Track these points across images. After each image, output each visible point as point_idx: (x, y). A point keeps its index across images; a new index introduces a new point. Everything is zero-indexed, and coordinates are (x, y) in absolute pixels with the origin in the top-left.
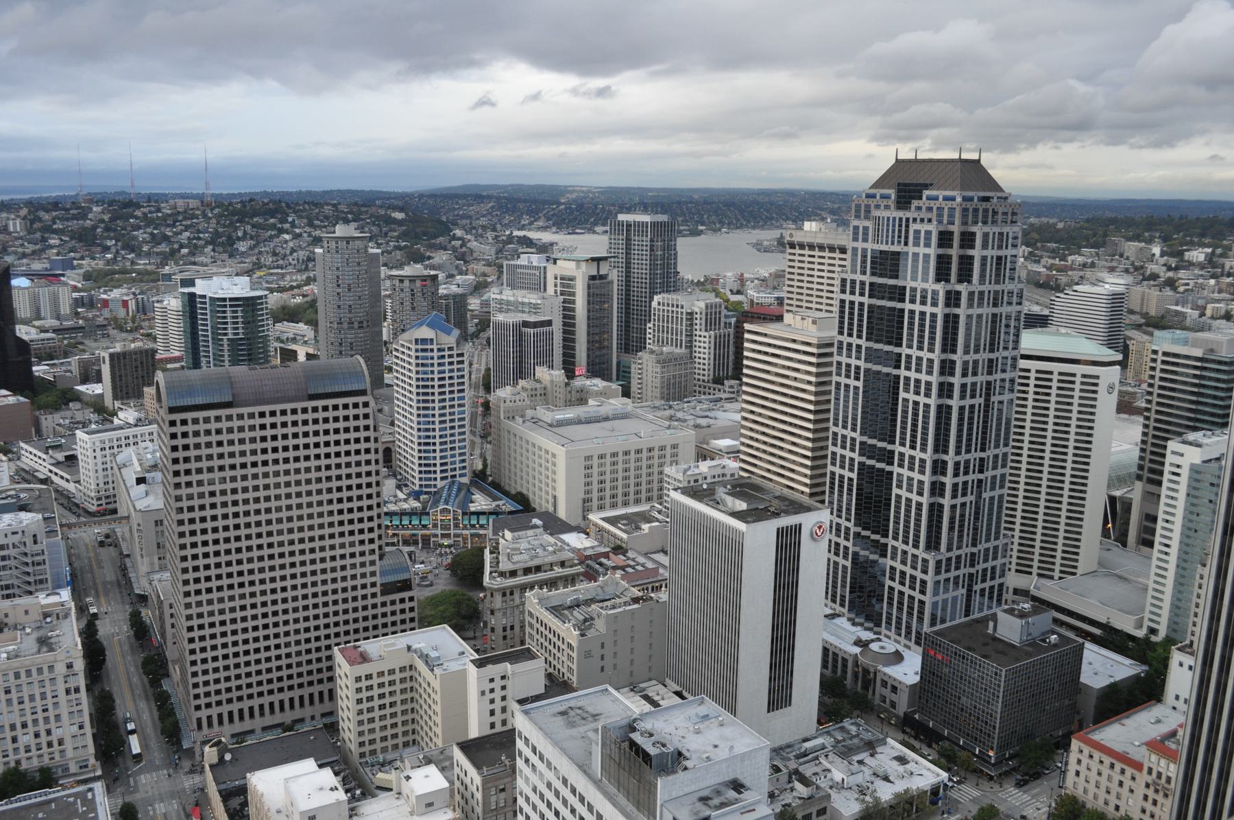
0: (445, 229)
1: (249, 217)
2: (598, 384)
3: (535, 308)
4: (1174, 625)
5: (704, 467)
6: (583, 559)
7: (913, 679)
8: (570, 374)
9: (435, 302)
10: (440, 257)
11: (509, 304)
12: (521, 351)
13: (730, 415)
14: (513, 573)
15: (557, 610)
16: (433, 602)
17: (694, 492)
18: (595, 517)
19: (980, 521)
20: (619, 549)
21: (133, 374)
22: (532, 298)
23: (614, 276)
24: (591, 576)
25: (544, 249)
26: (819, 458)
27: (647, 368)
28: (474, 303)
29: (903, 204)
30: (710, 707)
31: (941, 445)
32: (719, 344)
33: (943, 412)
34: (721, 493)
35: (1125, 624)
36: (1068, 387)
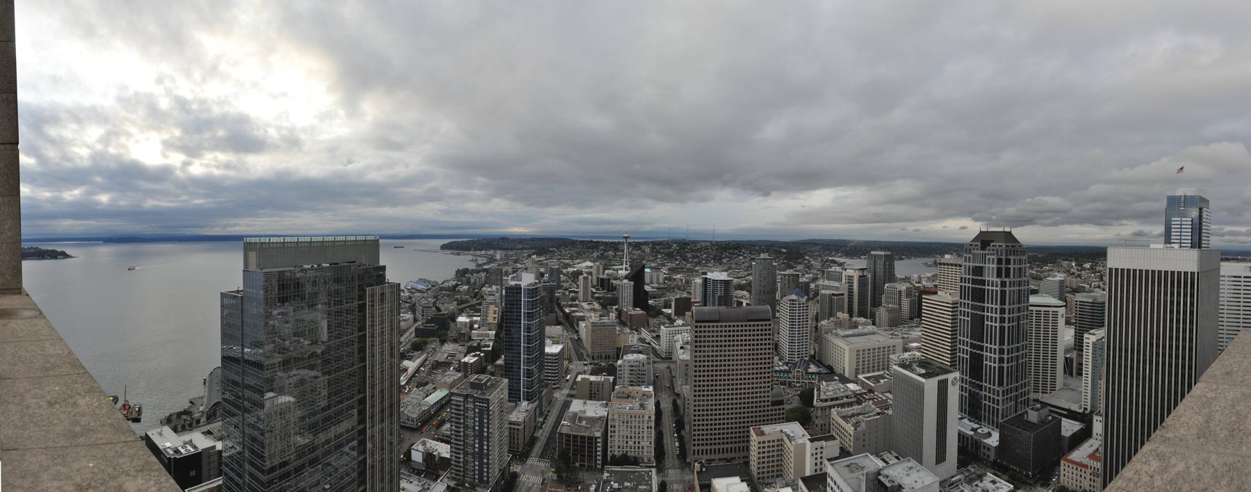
0: (802, 256)
1: (727, 250)
2: (863, 320)
3: (837, 288)
4: (1093, 406)
5: (906, 355)
6: (855, 394)
7: (996, 444)
8: (851, 316)
9: (798, 284)
10: (800, 267)
11: (827, 287)
12: (830, 306)
13: (916, 333)
14: (826, 400)
15: (844, 418)
16: (792, 411)
17: (903, 366)
18: (860, 377)
19: (1019, 372)
20: (871, 391)
21: (683, 306)
22: (836, 284)
23: (869, 276)
24: (859, 403)
25: (840, 265)
26: (953, 350)
27: (882, 313)
28: (812, 286)
30: (913, 463)
31: (1002, 343)
32: (912, 303)
34: (914, 366)
35: (1075, 408)
36: (1047, 316)
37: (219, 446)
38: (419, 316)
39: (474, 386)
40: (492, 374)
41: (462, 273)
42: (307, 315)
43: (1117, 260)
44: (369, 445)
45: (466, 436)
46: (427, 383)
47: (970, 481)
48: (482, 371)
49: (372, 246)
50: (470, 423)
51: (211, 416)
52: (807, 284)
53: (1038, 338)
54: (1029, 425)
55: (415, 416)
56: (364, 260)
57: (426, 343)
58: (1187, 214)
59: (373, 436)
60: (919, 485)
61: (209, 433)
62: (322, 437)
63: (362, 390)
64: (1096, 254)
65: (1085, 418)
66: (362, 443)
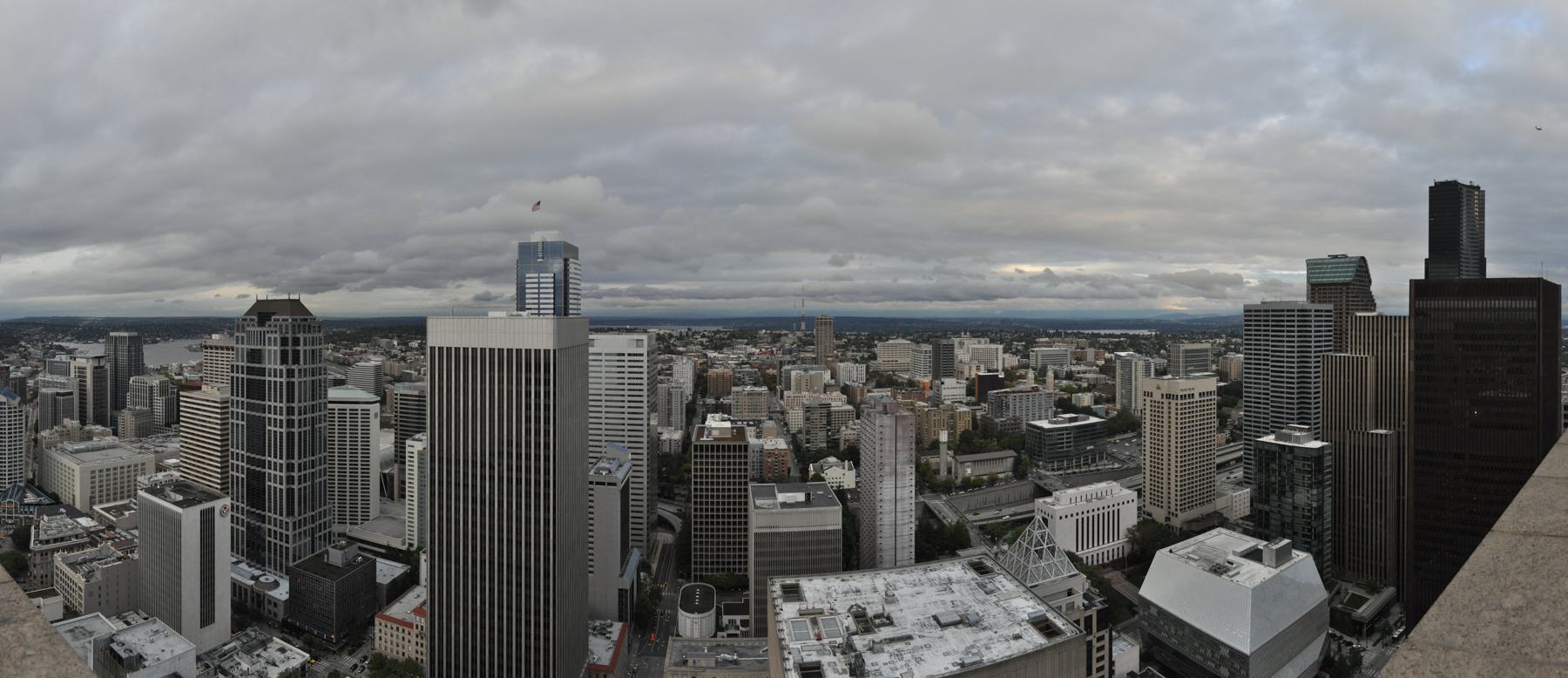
0: (16, 341)
2: (99, 428)
3: (63, 385)
5: (160, 476)
6: (89, 532)
7: (285, 597)
8: (83, 422)
10: (12, 357)
11: (49, 383)
12: (55, 410)
13: (174, 445)
14: (47, 542)
15: (72, 565)
17: (152, 490)
18: (97, 508)
20: (111, 527)
22: (62, 379)
23: (108, 366)
24: (93, 544)
25: (70, 352)
26: (224, 467)
27: (127, 418)
28: (31, 383)
29: (261, 324)
31: (290, 455)
32: (168, 404)
33: (290, 435)
34: (168, 490)
35: (396, 544)
36: (353, 417)
43: (440, 335)
47: (249, 650)
52: (23, 381)
53: (342, 448)
54: (332, 570)
58: (548, 268)
60: (167, 656)
64: (413, 328)
65: (407, 557)
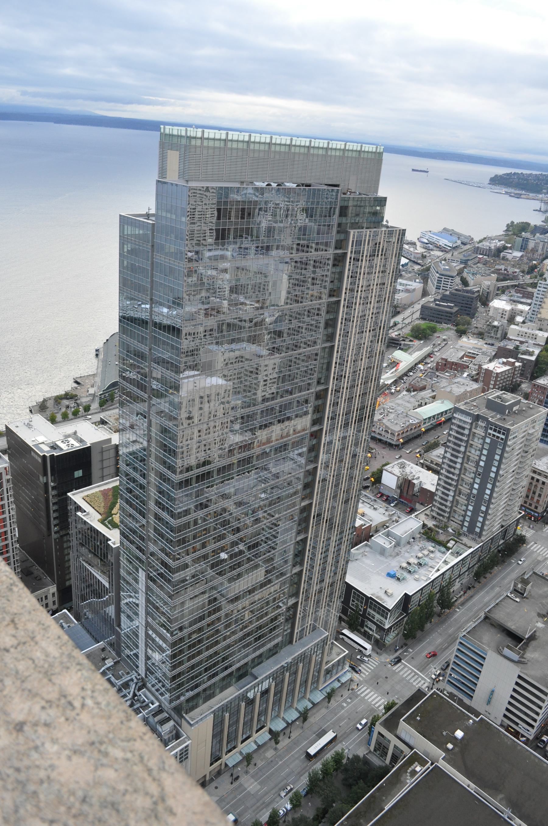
37: (116, 439)
38: (431, 287)
39: (491, 405)
40: (527, 396)
41: (517, 230)
42: (254, 262)
44: (322, 457)
45: (463, 470)
46: (423, 388)
48: (513, 388)
49: (370, 163)
50: (474, 454)
51: (105, 401)
55: (397, 429)
56: (353, 185)
57: (434, 330)
59: (330, 443)
61: (103, 422)
62: (262, 435)
63: (323, 380)
66: (314, 450)
